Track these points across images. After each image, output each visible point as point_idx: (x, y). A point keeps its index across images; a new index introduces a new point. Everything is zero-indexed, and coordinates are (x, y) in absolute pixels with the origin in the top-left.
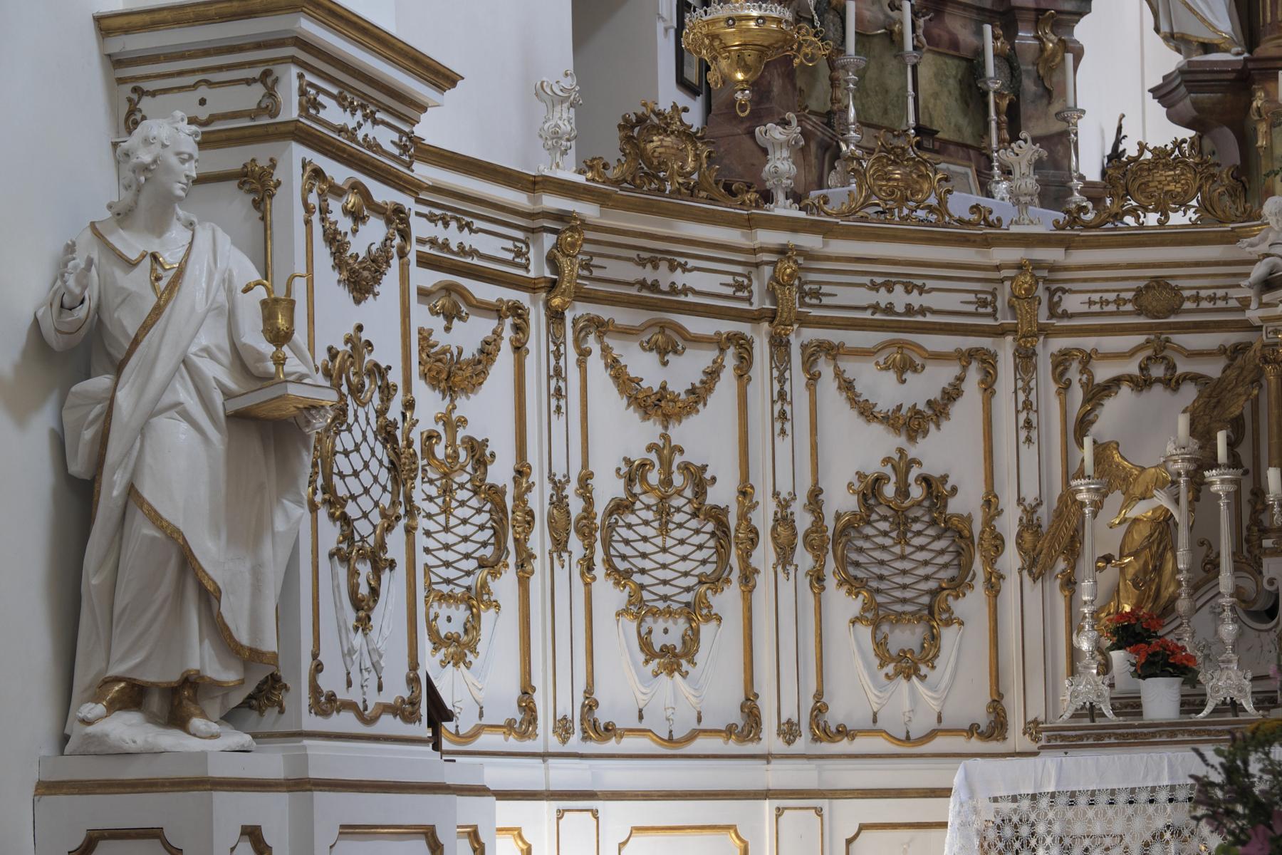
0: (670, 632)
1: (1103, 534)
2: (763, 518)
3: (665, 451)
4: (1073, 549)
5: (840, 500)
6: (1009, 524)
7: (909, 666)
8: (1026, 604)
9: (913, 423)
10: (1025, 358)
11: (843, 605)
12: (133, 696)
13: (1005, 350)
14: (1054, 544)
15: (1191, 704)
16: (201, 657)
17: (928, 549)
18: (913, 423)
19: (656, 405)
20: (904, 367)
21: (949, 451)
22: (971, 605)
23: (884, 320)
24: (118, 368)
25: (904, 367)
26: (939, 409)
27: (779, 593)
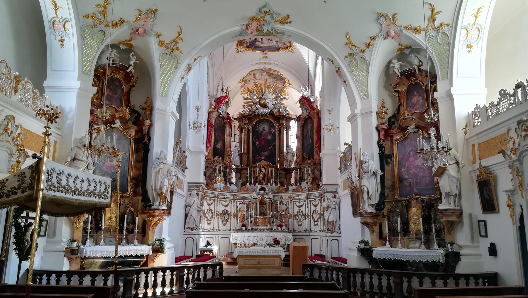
0: (209, 222)
1: (239, 216)
2: (215, 213)
3: (210, 208)
4: (237, 216)
5: (221, 212)
6: (232, 214)
7: (225, 225)
8: (233, 220)
9: (226, 206)
10: (234, 201)
11: (220, 220)
12: (189, 228)
13: (233, 201)
14: (235, 216)
15: (246, 229)
16: (194, 226)
17: (226, 215)
18: (226, 206)
19: (209, 205)
20: (225, 202)
21: (228, 208)
22: (229, 220)
23: (224, 198)
24: (190, 207)
25: (225, 202)
26: (228, 205)
27: (216, 219)
